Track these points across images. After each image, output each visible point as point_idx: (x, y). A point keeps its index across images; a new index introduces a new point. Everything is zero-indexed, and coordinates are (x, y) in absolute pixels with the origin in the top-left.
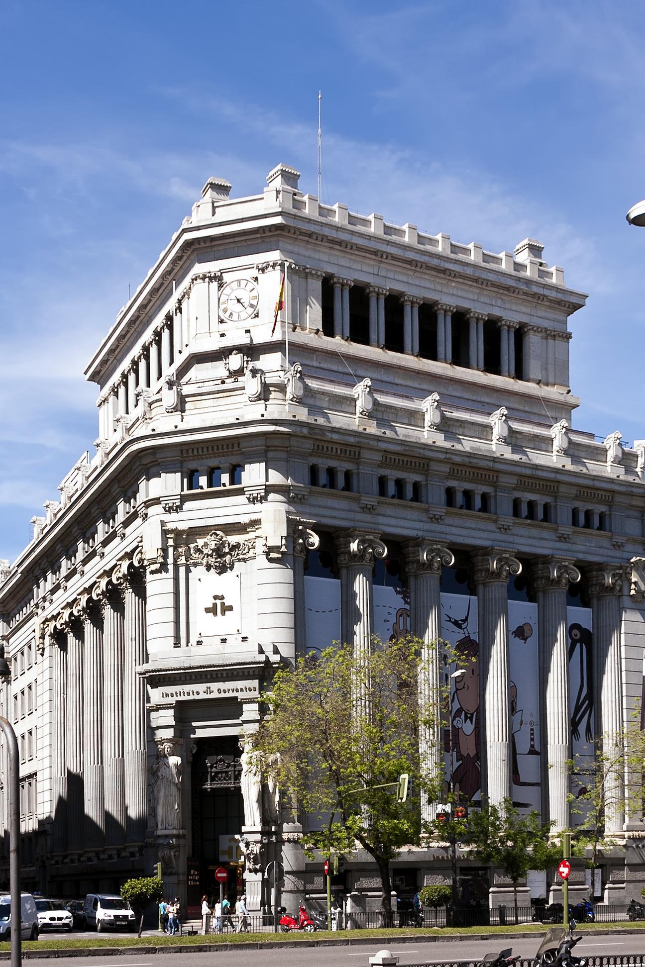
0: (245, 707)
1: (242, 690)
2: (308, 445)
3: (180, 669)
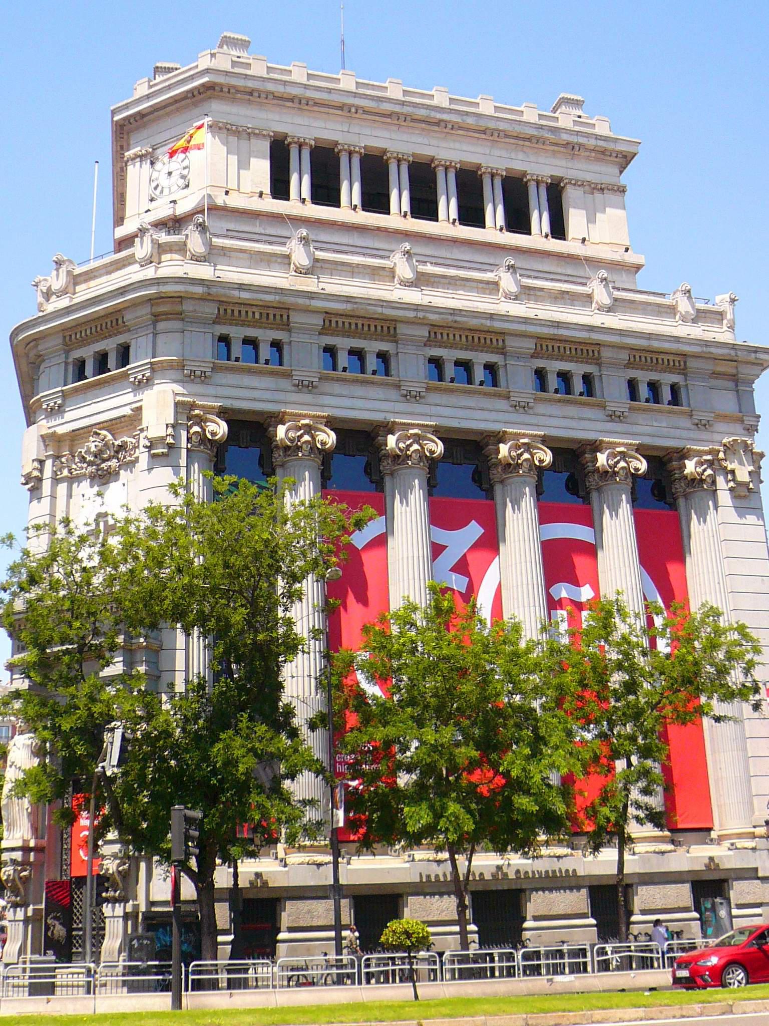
2: (210, 310)
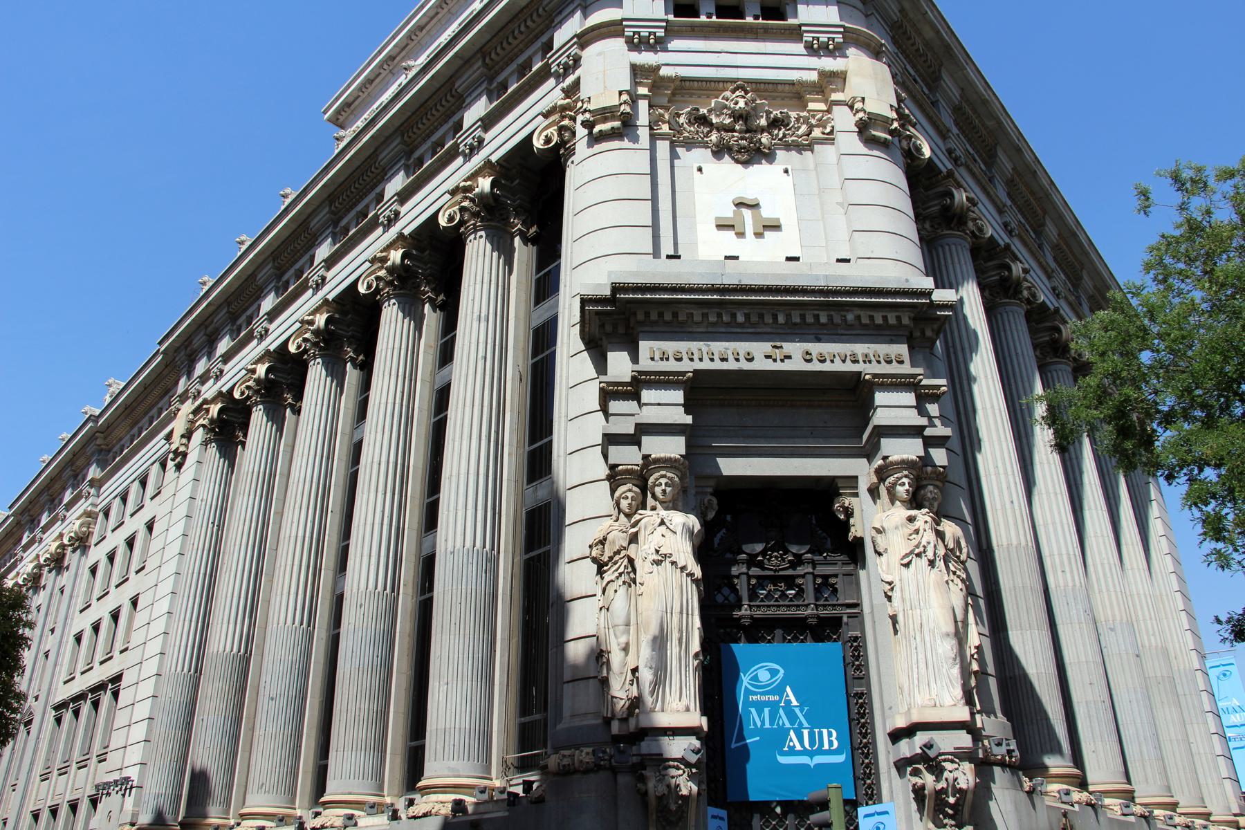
0: (880, 398)
1: (867, 360)
3: (713, 289)
